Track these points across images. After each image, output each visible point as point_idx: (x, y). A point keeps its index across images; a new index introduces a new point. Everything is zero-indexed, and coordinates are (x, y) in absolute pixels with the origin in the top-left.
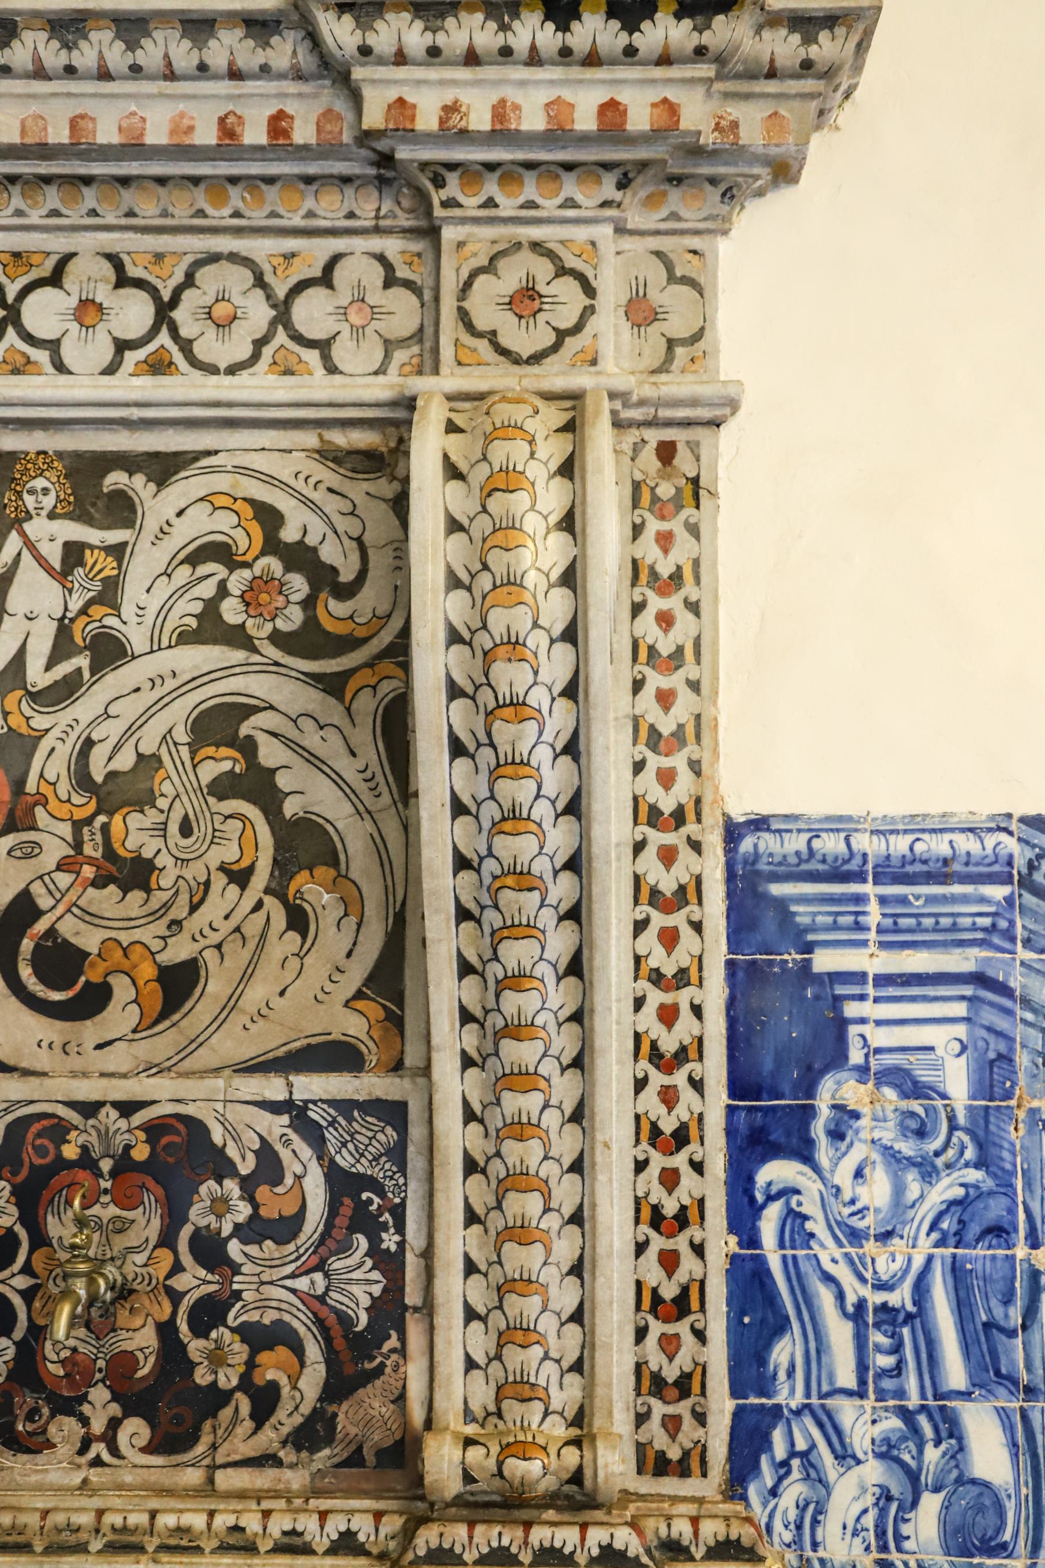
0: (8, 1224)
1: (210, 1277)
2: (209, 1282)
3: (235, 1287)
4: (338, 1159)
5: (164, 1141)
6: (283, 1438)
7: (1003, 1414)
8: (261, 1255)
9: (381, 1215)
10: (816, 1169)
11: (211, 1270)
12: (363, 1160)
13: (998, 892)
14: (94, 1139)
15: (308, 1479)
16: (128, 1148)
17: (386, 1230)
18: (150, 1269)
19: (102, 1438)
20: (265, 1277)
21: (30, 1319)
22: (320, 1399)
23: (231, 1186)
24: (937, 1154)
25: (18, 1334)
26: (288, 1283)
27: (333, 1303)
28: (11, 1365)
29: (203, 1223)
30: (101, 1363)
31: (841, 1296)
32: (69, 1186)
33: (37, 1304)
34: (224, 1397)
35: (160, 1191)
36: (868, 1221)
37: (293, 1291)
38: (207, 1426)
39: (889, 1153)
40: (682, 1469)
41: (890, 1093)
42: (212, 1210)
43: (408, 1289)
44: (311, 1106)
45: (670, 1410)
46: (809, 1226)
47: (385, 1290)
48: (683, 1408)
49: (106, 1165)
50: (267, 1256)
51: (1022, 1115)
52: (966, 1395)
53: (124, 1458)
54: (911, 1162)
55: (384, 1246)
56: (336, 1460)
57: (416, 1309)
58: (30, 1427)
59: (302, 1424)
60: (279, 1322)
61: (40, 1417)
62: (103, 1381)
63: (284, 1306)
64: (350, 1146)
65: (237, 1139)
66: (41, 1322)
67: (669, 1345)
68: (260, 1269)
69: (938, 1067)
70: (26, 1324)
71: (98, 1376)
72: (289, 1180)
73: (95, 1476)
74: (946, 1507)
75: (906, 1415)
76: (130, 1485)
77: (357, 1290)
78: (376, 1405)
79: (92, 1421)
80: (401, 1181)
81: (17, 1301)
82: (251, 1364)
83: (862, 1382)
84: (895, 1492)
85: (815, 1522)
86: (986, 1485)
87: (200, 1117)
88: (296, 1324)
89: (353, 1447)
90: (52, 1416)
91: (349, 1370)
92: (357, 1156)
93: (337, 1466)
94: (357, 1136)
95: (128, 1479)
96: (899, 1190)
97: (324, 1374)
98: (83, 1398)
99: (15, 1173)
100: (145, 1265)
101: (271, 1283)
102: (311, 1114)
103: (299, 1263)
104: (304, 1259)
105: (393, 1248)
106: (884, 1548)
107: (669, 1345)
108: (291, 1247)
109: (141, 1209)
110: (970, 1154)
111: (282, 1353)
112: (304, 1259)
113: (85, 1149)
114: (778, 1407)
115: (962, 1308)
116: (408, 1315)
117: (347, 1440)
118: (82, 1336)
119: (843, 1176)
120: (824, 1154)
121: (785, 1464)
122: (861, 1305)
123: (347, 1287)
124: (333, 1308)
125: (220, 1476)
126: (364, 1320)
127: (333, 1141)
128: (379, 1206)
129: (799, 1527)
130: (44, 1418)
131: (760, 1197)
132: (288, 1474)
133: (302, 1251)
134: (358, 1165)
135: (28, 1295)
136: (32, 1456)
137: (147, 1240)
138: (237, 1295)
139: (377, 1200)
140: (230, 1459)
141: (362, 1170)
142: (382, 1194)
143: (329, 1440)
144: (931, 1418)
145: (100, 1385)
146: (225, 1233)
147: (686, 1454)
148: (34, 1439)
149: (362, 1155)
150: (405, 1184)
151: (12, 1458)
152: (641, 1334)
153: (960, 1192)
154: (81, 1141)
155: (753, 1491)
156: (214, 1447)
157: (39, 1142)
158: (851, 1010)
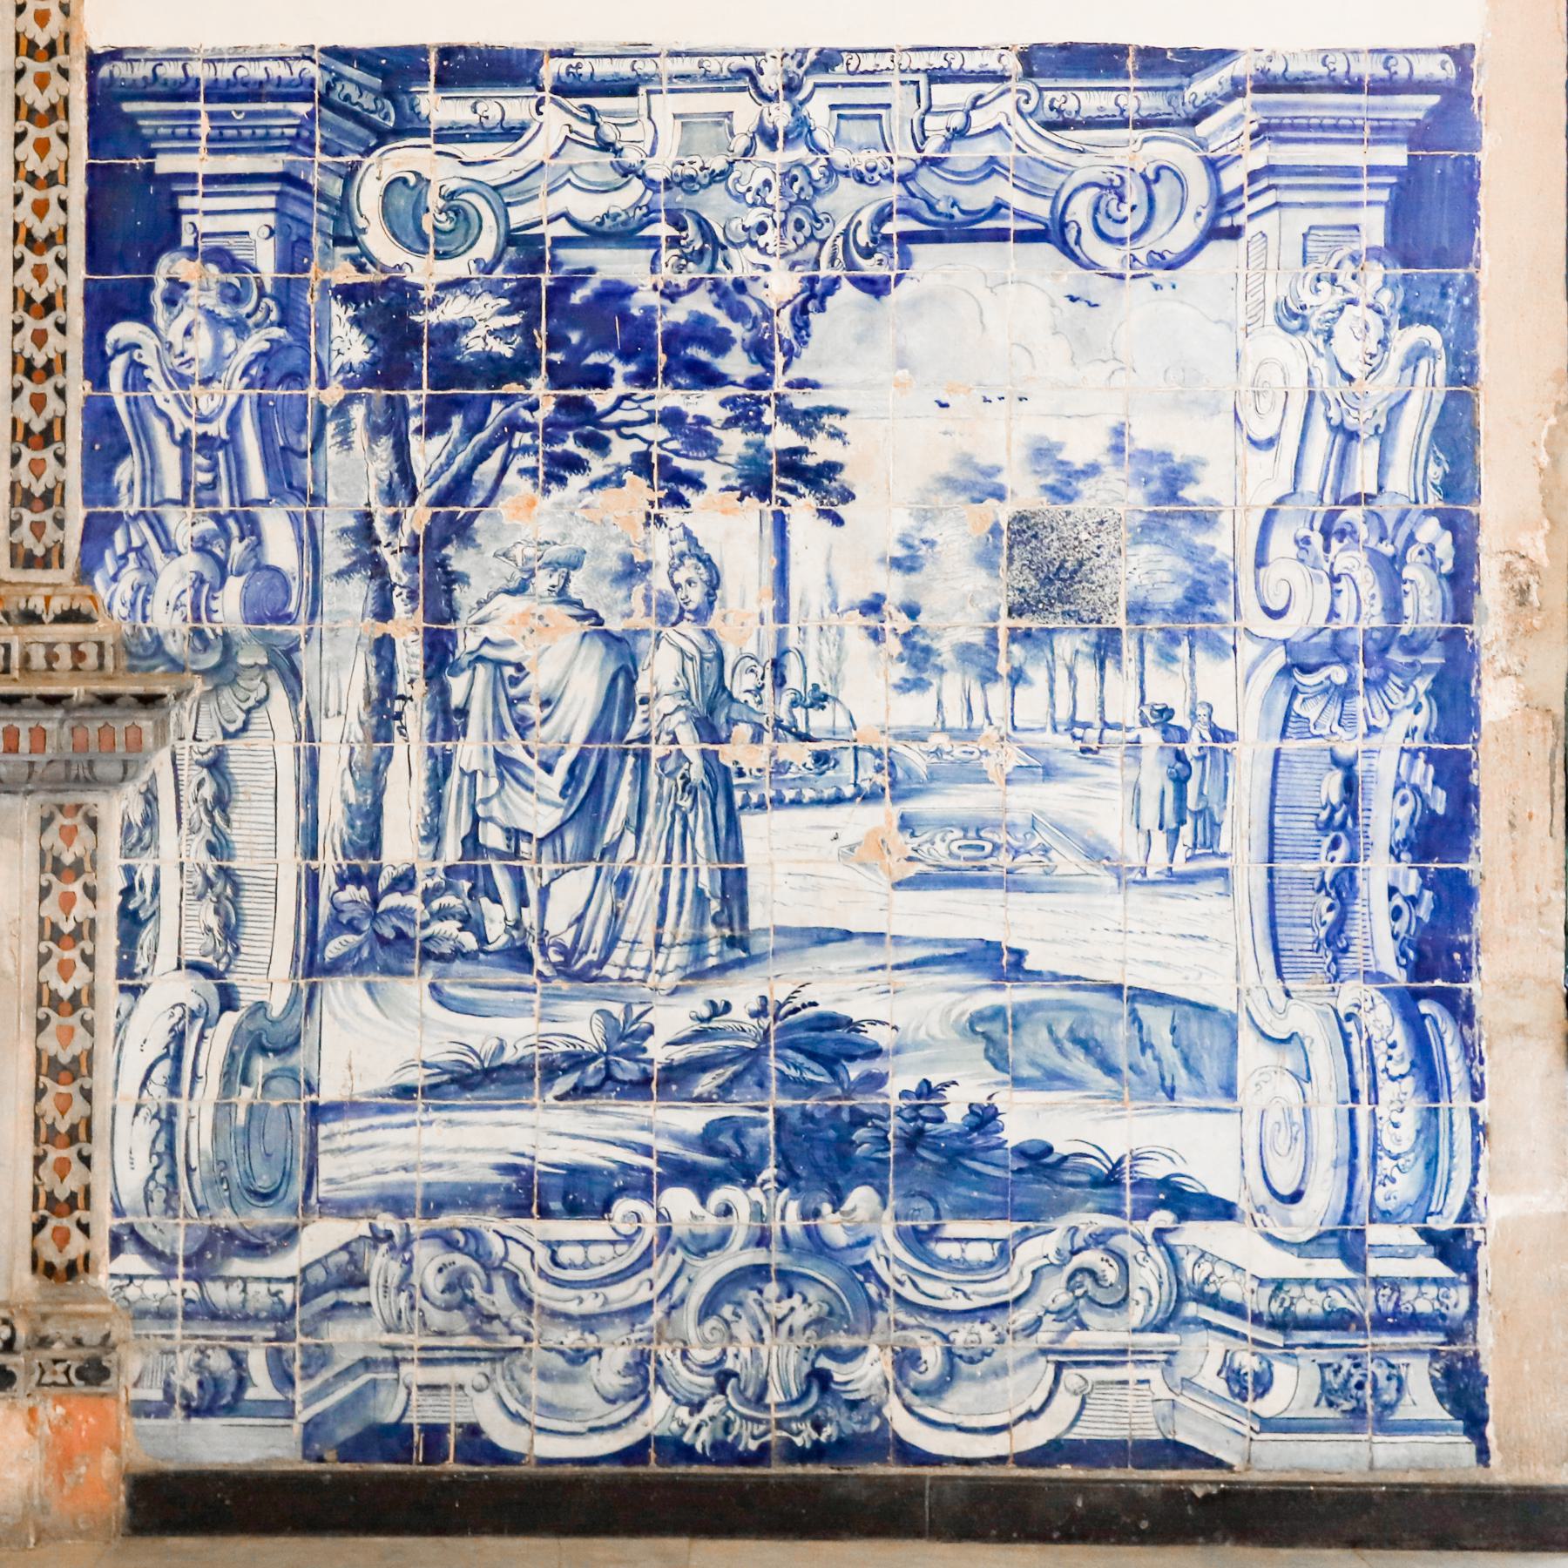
7: (294, 518)
10: (154, 329)
13: (302, 108)
24: (249, 316)
31: (171, 427)
36: (194, 370)
39: (210, 315)
40: (45, 563)
41: (213, 269)
45: (37, 517)
46: (147, 373)
48: (47, 516)
51: (316, 285)
52: (264, 503)
54: (228, 323)
67: (37, 468)
69: (251, 247)
74: (246, 587)
75: (218, 519)
83: (186, 493)
84: (207, 576)
85: (146, 600)
86: (276, 570)
96: (218, 344)
106: (198, 619)
107: (37, 468)
110: (274, 316)
114: (120, 514)
115: (265, 434)
119: (175, 334)
120: (160, 314)
121: (124, 557)
122: (186, 435)
129: (133, 605)
131: (109, 351)
144: (237, 521)
147: (48, 551)
152: (15, 459)
153: (267, 345)
155: (98, 579)
158: (185, 203)
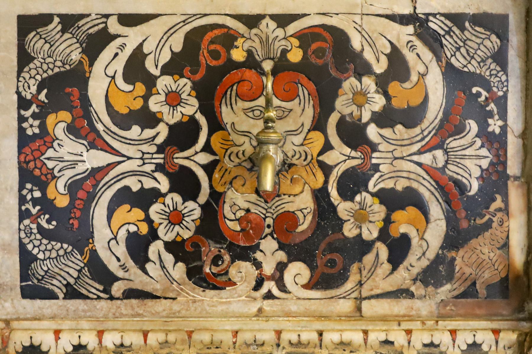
0: (191, 113)
1: (354, 154)
2: (353, 158)
3: (374, 161)
4: (453, 60)
5: (314, 46)
6: (414, 277)
8: (393, 136)
9: (488, 105)
11: (354, 147)
12: (473, 62)
14: (257, 45)
15: (434, 307)
16: (284, 52)
17: (492, 117)
18: (305, 148)
19: (272, 278)
20: (397, 154)
21: (211, 187)
22: (442, 248)
23: (369, 82)
25: (203, 198)
26: (415, 158)
27: (451, 174)
28: (198, 223)
29: (347, 111)
30: (269, 221)
32: (238, 83)
33: (216, 175)
34: (366, 246)
35: (312, 86)
37: (420, 164)
38: (354, 267)
42: (354, 101)
43: (509, 163)
44: (431, 18)
47: (491, 164)
49: (268, 66)
50: (398, 137)
53: (290, 293)
55: (490, 129)
56: (456, 293)
57: (516, 178)
58: (215, 270)
59: (428, 266)
60: (409, 189)
61: (223, 262)
62: (271, 234)
63: (412, 176)
64: (463, 50)
65: (372, 45)
66: (220, 189)
68: (394, 147)
70: (208, 191)
71: (267, 231)
72: (414, 78)
73: (267, 305)
76: (295, 312)
77: (468, 163)
78: (486, 250)
79: (264, 265)
80: (504, 78)
81: (201, 174)
82: (387, 221)
87: (341, 27)
88: (422, 190)
89: (469, 283)
90: (233, 261)
91: (464, 224)
92: (468, 58)
93: (457, 297)
94: (468, 42)
95: (293, 307)
97: (444, 228)
98: (256, 248)
99: (194, 72)
100: (302, 145)
101: (402, 158)
102: (431, 24)
103: (424, 143)
104: (427, 139)
105: (498, 131)
108: (417, 130)
109: (297, 101)
111: (412, 211)
112: (427, 139)
113: (250, 53)
116: (509, 183)
117: (464, 278)
118: (253, 200)
123: (462, 161)
124: (451, 178)
125: (366, 305)
126: (475, 187)
127: (449, 46)
128: (487, 98)
130: (226, 263)
132: (417, 304)
133: (425, 133)
134: (469, 66)
135: (209, 169)
136: (217, 292)
137: (303, 125)
138: (376, 168)
139: (484, 93)
140: (373, 293)
141: (472, 69)
142: (489, 90)
143: (450, 277)
145: (269, 237)
146: (365, 120)
148: (218, 279)
149: (473, 58)
150: (507, 81)
151: (202, 293)
154: (246, 46)
156: (360, 284)
157: (213, 47)
